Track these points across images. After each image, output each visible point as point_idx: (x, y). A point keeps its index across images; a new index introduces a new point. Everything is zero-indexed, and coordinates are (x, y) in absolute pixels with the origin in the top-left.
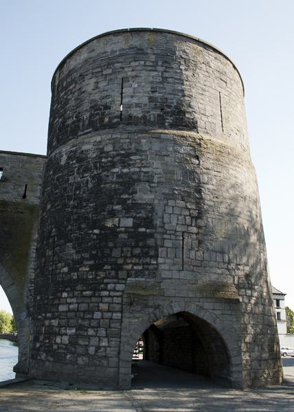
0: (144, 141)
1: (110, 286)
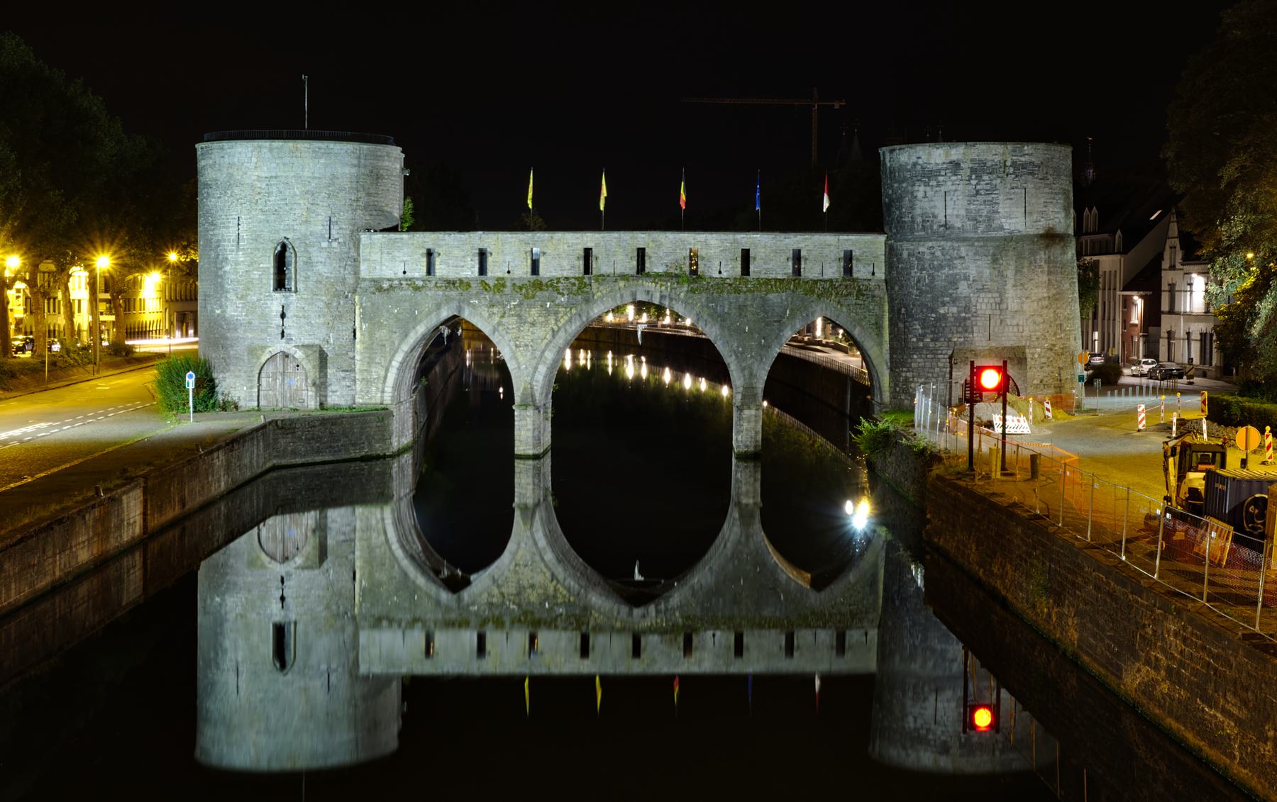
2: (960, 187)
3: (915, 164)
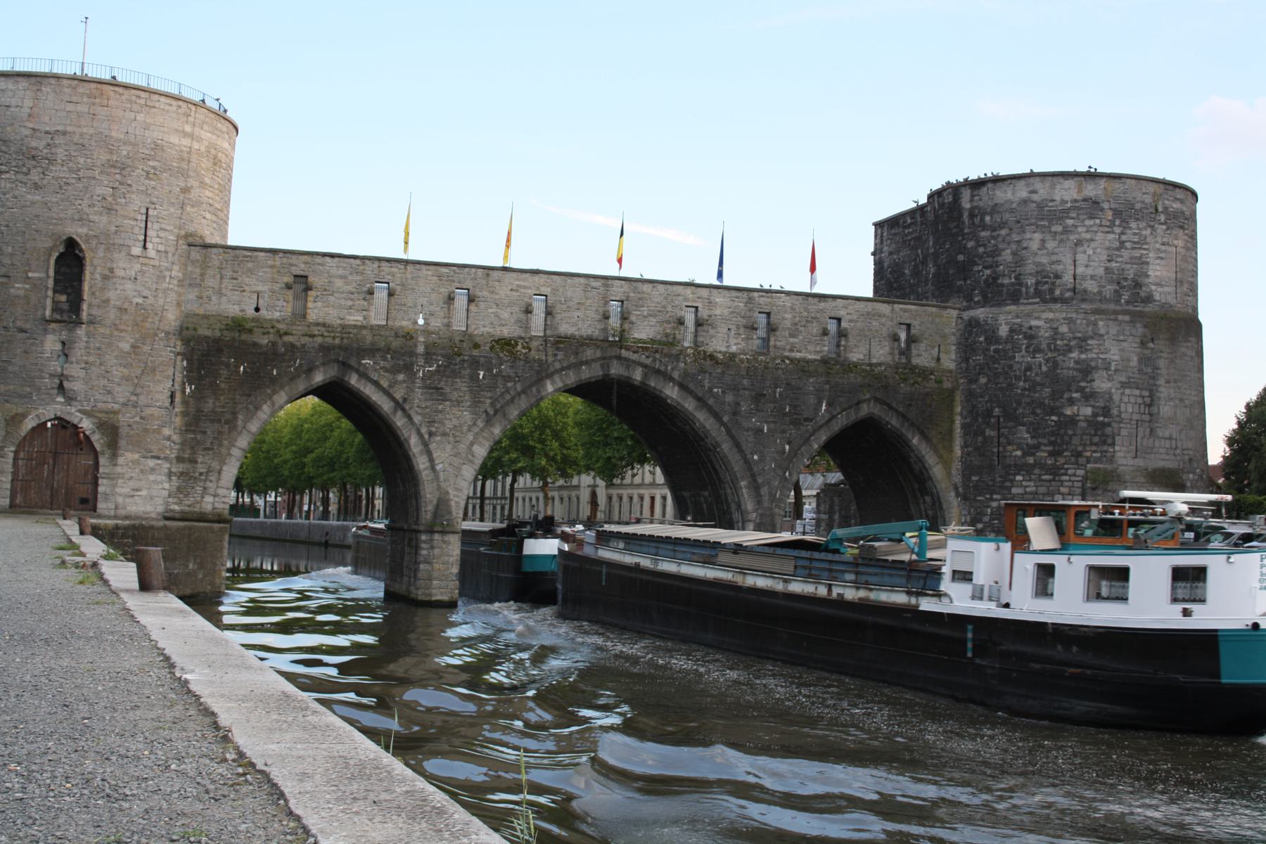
0: (1101, 323)
1: (1070, 472)
2: (1100, 236)
3: (1025, 202)
